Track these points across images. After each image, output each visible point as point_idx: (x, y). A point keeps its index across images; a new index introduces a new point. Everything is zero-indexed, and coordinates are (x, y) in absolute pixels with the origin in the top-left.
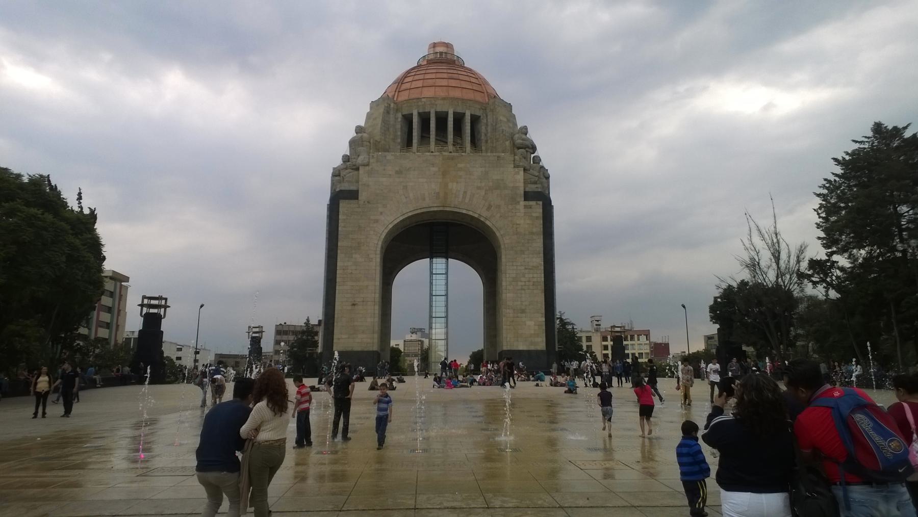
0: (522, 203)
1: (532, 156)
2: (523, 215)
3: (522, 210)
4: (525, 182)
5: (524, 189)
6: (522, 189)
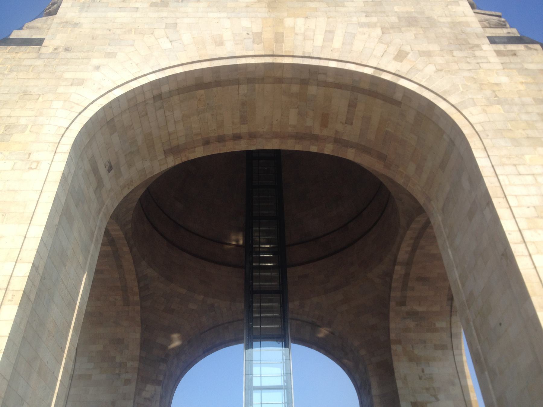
0: (488, 48)
2: (500, 67)
3: (494, 59)
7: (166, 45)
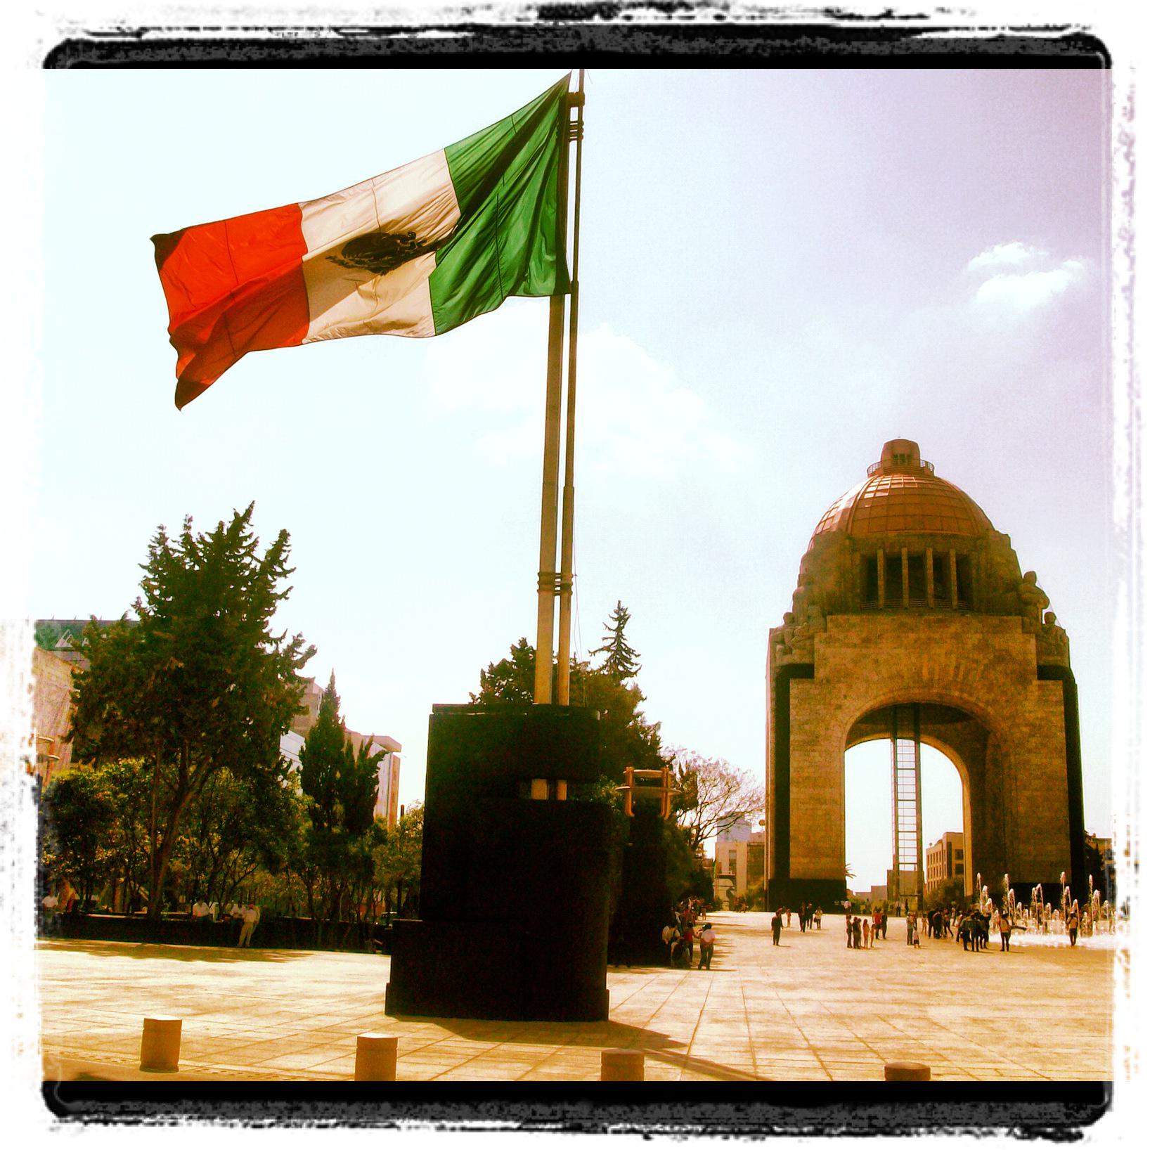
0: (1036, 682)
1: (1044, 611)
4: (1039, 653)
6: (1034, 663)
7: (876, 678)
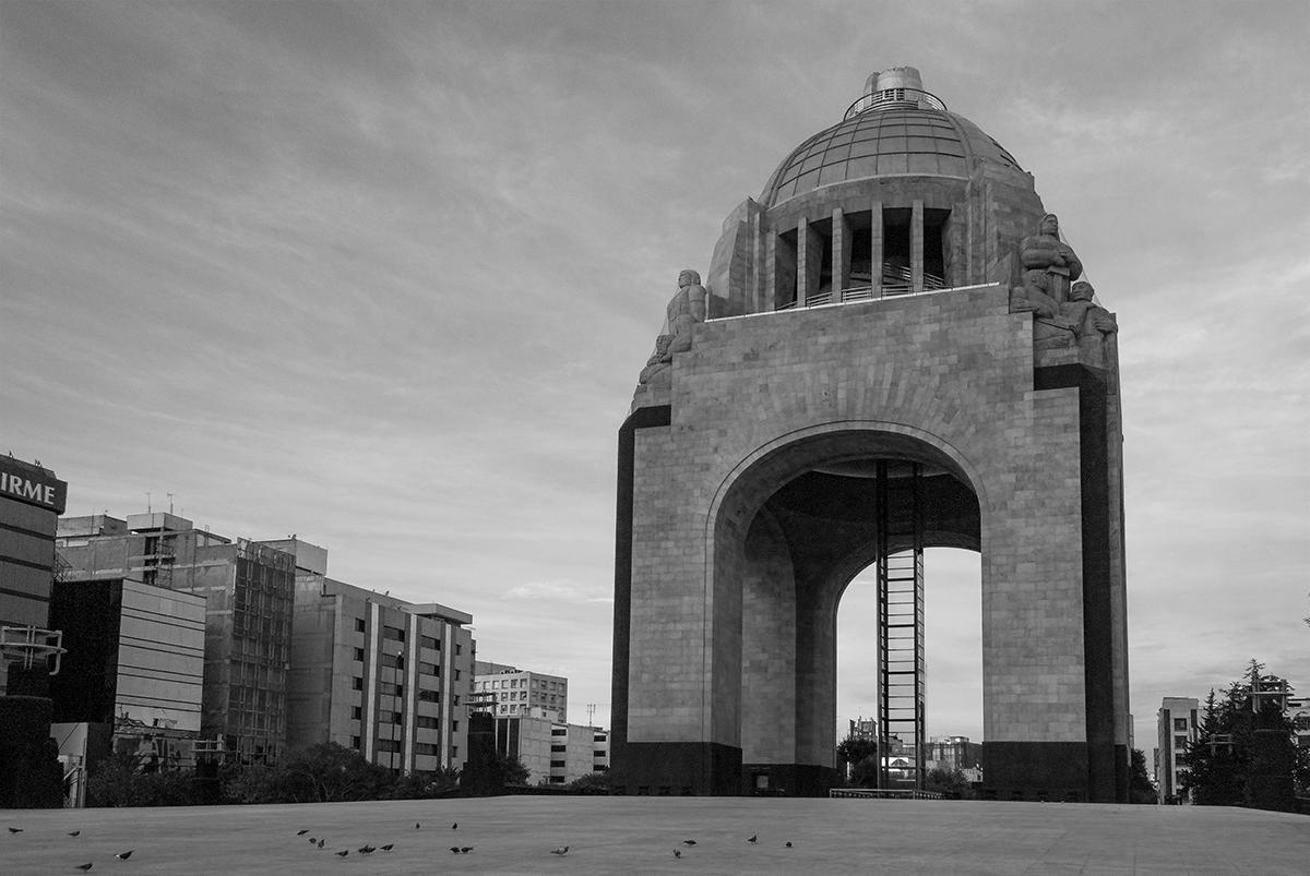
0: (1029, 396)
1: (1072, 283)
3: (1030, 414)
5: (1036, 361)
